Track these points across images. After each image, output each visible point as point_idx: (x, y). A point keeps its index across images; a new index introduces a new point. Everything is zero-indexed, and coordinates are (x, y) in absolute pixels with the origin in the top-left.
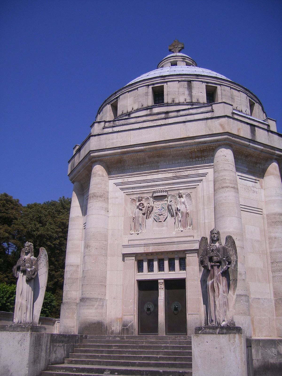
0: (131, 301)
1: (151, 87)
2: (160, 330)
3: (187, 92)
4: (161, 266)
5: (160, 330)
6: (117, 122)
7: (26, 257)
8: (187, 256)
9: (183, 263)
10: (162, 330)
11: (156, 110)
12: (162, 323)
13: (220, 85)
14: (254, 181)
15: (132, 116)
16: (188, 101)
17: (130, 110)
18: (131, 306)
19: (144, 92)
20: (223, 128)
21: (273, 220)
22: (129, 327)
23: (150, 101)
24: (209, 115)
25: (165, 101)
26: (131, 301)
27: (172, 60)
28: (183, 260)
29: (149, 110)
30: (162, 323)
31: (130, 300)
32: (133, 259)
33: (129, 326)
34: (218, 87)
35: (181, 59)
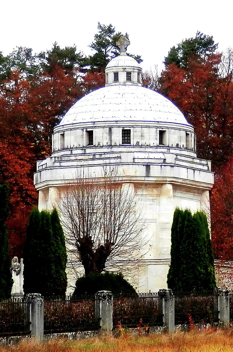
1: (85, 130)
3: (108, 137)
6: (63, 158)
7: (15, 264)
11: (88, 151)
13: (133, 126)
14: (152, 200)
15: (74, 152)
16: (109, 144)
17: (72, 147)
19: (81, 134)
20: (125, 173)
21: (162, 227)
23: (84, 142)
24: (118, 161)
25: (94, 144)
27: (114, 70)
29: (83, 150)
34: (132, 129)
35: (122, 70)
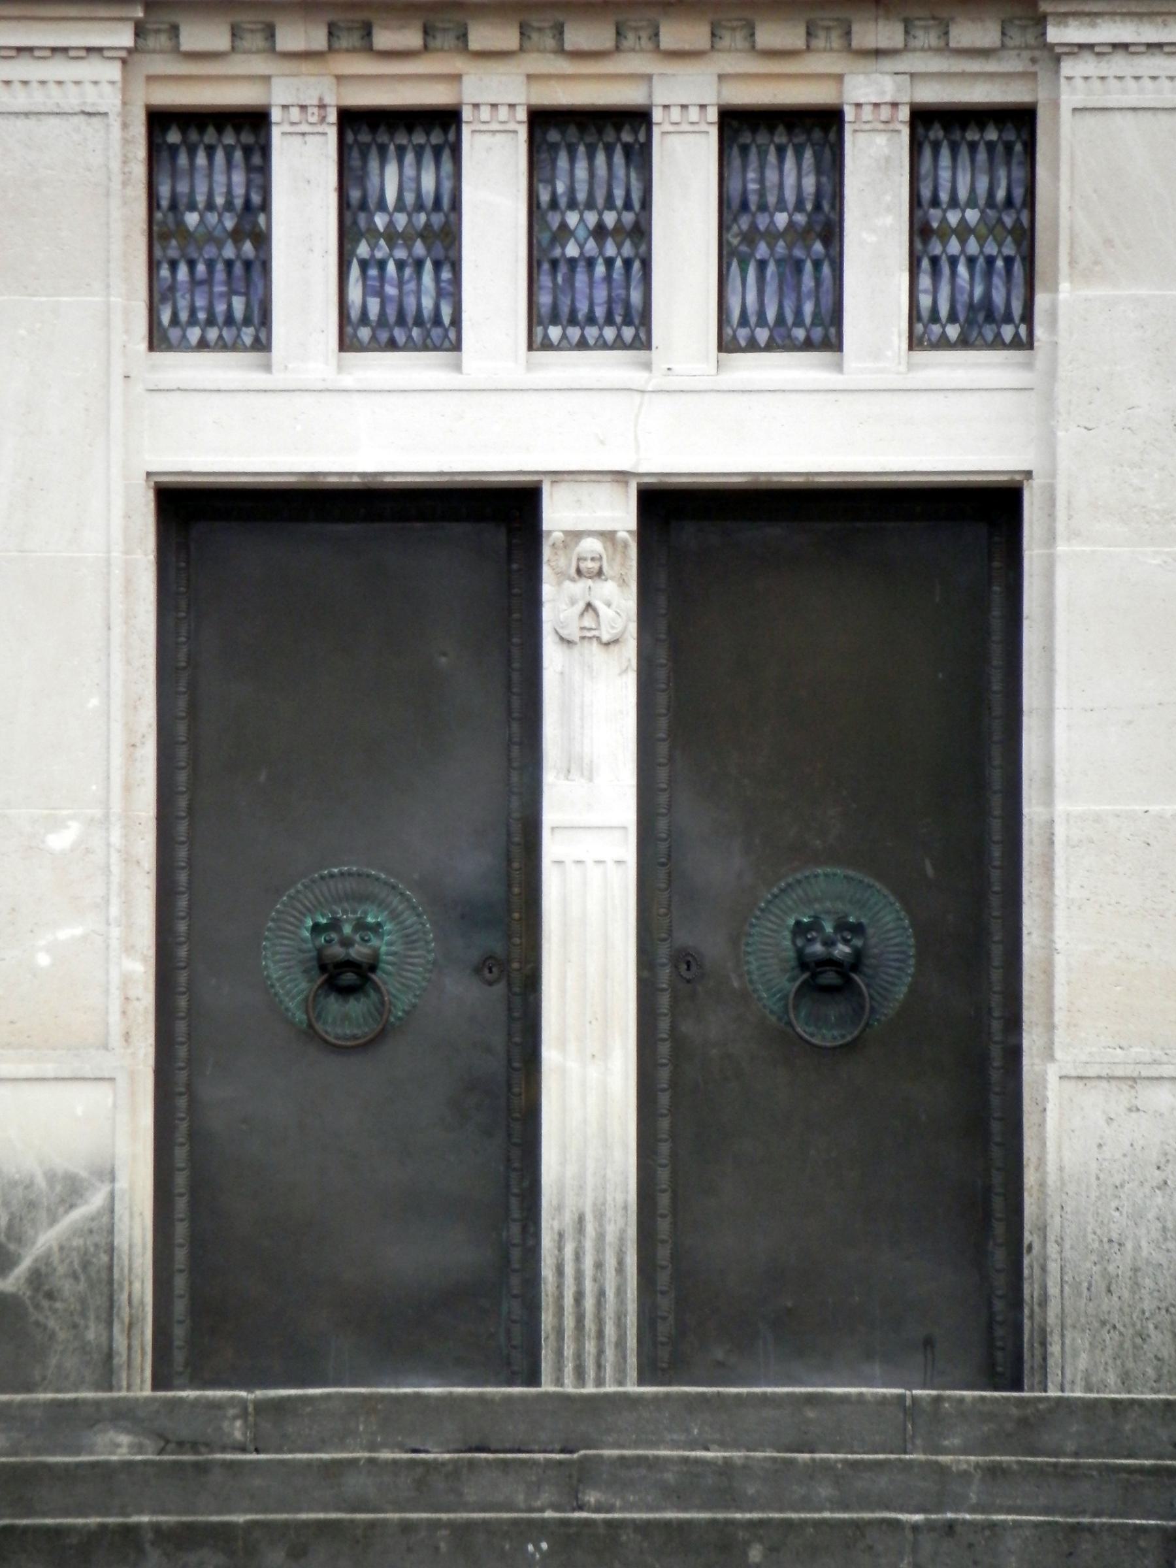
0: (60, 840)
2: (569, 1322)
4: (572, 250)
5: (569, 1322)
8: (1069, 98)
9: (972, 202)
10: (600, 1335)
12: (600, 1215)
18: (64, 934)
22: (36, 1277)
26: (60, 840)
28: (973, 147)
30: (600, 1215)
31: (56, 824)
32: (93, 98)
33: (46, 1258)
